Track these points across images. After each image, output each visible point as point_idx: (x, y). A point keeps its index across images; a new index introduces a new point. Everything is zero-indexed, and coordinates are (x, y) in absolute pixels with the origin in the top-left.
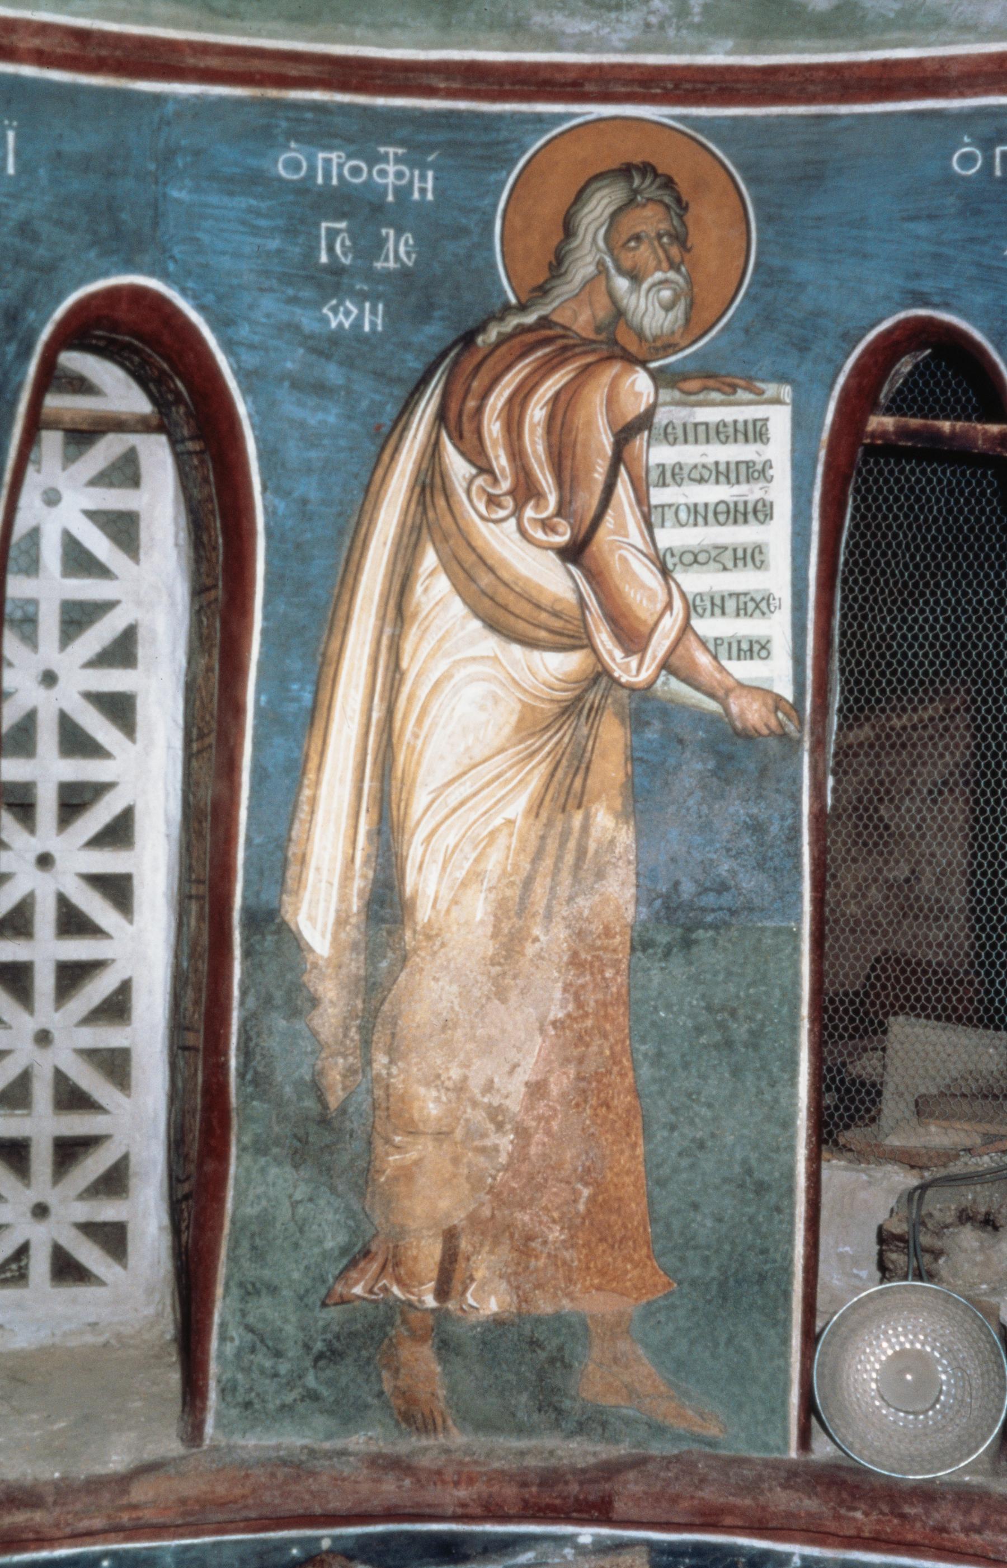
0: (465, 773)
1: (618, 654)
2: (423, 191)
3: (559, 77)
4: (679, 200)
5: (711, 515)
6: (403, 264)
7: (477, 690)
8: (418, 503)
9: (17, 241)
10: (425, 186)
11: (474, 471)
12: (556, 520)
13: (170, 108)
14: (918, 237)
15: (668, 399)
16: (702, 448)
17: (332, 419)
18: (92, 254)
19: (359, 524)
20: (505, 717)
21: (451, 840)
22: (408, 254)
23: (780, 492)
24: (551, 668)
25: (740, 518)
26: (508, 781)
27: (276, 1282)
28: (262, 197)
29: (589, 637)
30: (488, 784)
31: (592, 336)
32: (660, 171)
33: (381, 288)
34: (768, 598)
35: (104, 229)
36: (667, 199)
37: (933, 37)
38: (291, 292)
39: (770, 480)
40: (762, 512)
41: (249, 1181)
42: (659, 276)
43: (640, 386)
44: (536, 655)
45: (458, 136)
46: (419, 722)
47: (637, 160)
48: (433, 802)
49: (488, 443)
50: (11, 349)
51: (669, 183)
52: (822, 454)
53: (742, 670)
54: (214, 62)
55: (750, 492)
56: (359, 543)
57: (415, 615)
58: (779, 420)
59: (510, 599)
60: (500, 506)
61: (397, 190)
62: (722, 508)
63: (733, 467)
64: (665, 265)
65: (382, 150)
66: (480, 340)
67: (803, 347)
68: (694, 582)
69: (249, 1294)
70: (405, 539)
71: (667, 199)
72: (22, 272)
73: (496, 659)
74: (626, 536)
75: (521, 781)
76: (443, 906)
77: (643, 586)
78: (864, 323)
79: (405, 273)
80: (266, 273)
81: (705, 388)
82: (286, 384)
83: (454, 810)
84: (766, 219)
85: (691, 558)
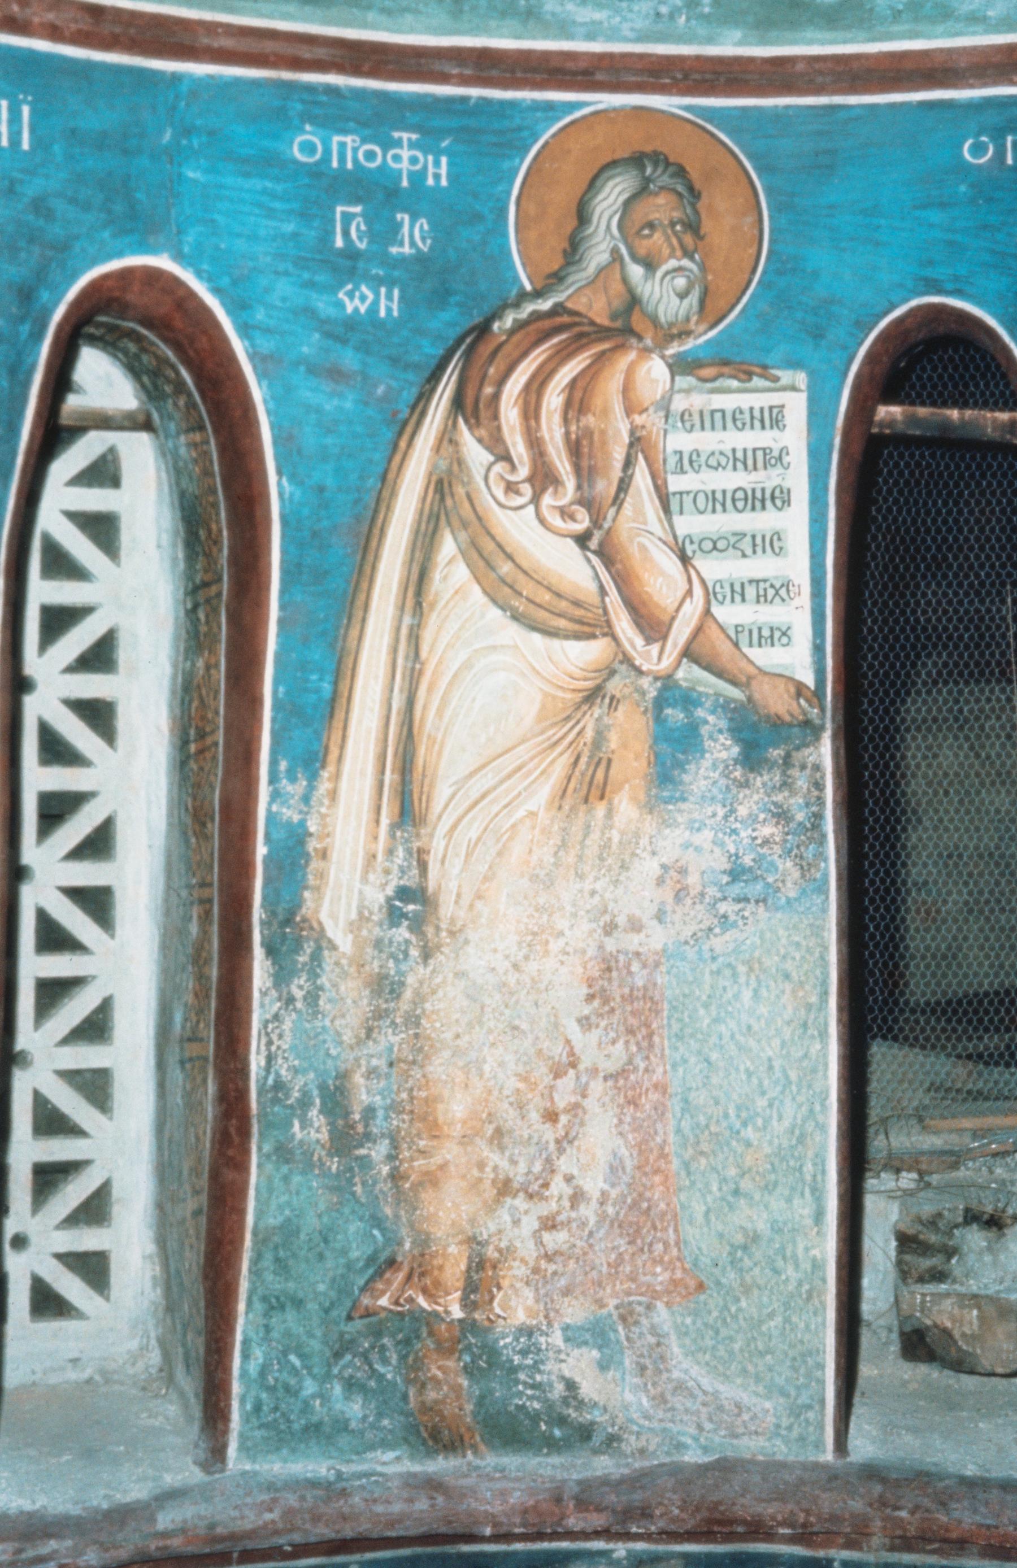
0: (483, 766)
1: (639, 641)
2: (437, 177)
3: (570, 65)
4: (691, 189)
5: (729, 502)
6: (418, 250)
8: (435, 492)
9: (31, 217)
10: (439, 172)
11: (492, 458)
12: (575, 507)
13: (184, 88)
14: (931, 226)
15: (685, 386)
16: (720, 435)
17: (348, 405)
18: (106, 234)
19: (376, 511)
20: (528, 704)
21: (473, 834)
22: (423, 239)
23: (797, 479)
25: (758, 504)
26: (530, 773)
27: (301, 1294)
28: (278, 180)
29: (609, 623)
30: (509, 776)
32: (671, 160)
33: (396, 273)
34: (787, 585)
35: (119, 208)
36: (680, 188)
37: (940, 29)
38: (306, 276)
40: (780, 498)
41: (271, 1190)
42: (673, 263)
43: (655, 372)
44: (556, 643)
45: (472, 122)
46: (440, 713)
47: (648, 149)
49: (505, 429)
50: (25, 329)
51: (681, 172)
52: (837, 441)
53: (765, 657)
54: (227, 43)
55: (768, 479)
56: (376, 531)
57: (432, 606)
58: (796, 407)
59: (528, 589)
60: (518, 493)
61: (411, 175)
62: (740, 495)
63: (750, 454)
64: (679, 253)
65: (396, 135)
66: (496, 326)
67: (817, 335)
68: (713, 568)
69: (273, 1308)
71: (680, 188)
72: (36, 250)
73: (516, 647)
74: (645, 523)
75: (542, 773)
76: (466, 900)
77: (662, 573)
78: (878, 309)
79: (420, 259)
80: (281, 256)
81: (721, 375)
82: (302, 368)
83: (476, 803)
84: (776, 209)
85: (710, 545)
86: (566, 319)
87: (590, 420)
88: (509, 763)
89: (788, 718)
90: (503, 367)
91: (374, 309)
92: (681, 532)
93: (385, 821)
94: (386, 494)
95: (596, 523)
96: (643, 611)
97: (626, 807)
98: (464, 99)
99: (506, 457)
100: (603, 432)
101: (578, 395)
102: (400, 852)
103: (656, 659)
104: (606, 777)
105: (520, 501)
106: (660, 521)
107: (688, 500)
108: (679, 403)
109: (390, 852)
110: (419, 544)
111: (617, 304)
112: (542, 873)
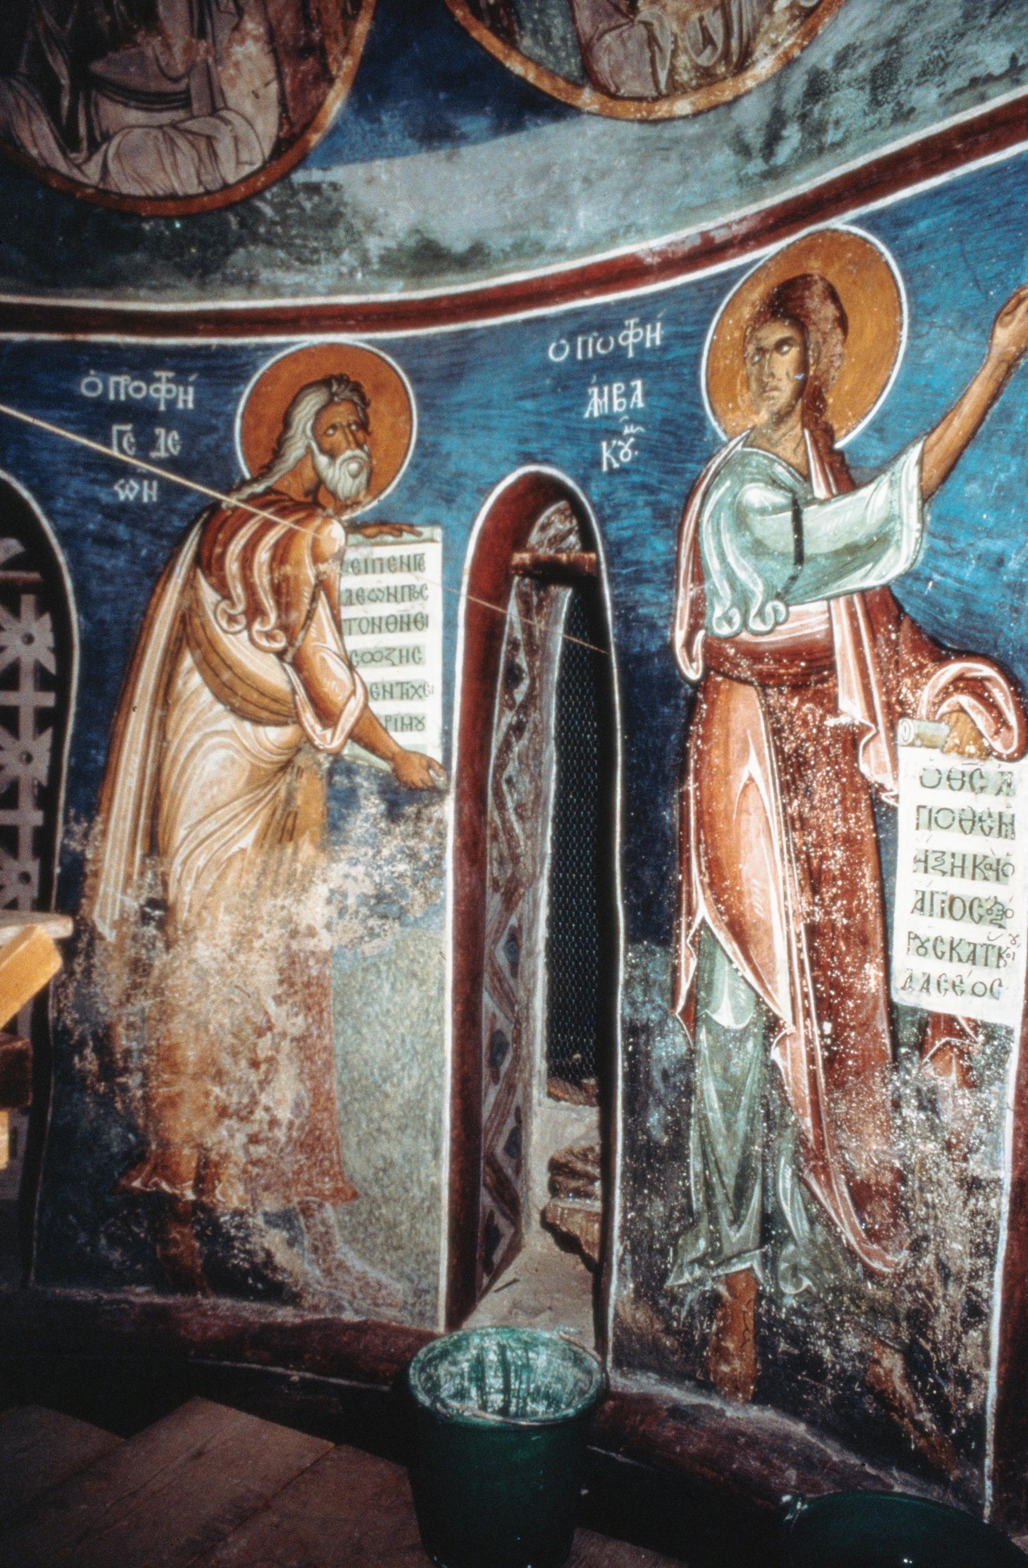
1: (318, 728)
4: (363, 398)
7: (221, 754)
10: (187, 399)
16: (377, 577)
21: (201, 863)
23: (434, 607)
28: (71, 409)
29: (298, 715)
31: (302, 499)
36: (356, 399)
37: (536, 261)
38: (92, 475)
39: (426, 599)
40: (419, 622)
42: (348, 453)
44: (261, 729)
45: (212, 362)
47: (336, 372)
49: (229, 580)
53: (404, 739)
58: (433, 554)
60: (236, 622)
65: (157, 374)
67: (449, 500)
68: (369, 674)
76: (196, 908)
77: (335, 678)
81: (381, 533)
84: (424, 407)
86: (273, 497)
87: (288, 569)
89: (420, 784)
93: (139, 852)
95: (291, 643)
97: (307, 849)
98: (208, 347)
100: (296, 578)
101: (280, 552)
102: (149, 875)
103: (330, 739)
108: (351, 555)
109: (142, 874)
111: (308, 485)
112: (248, 892)
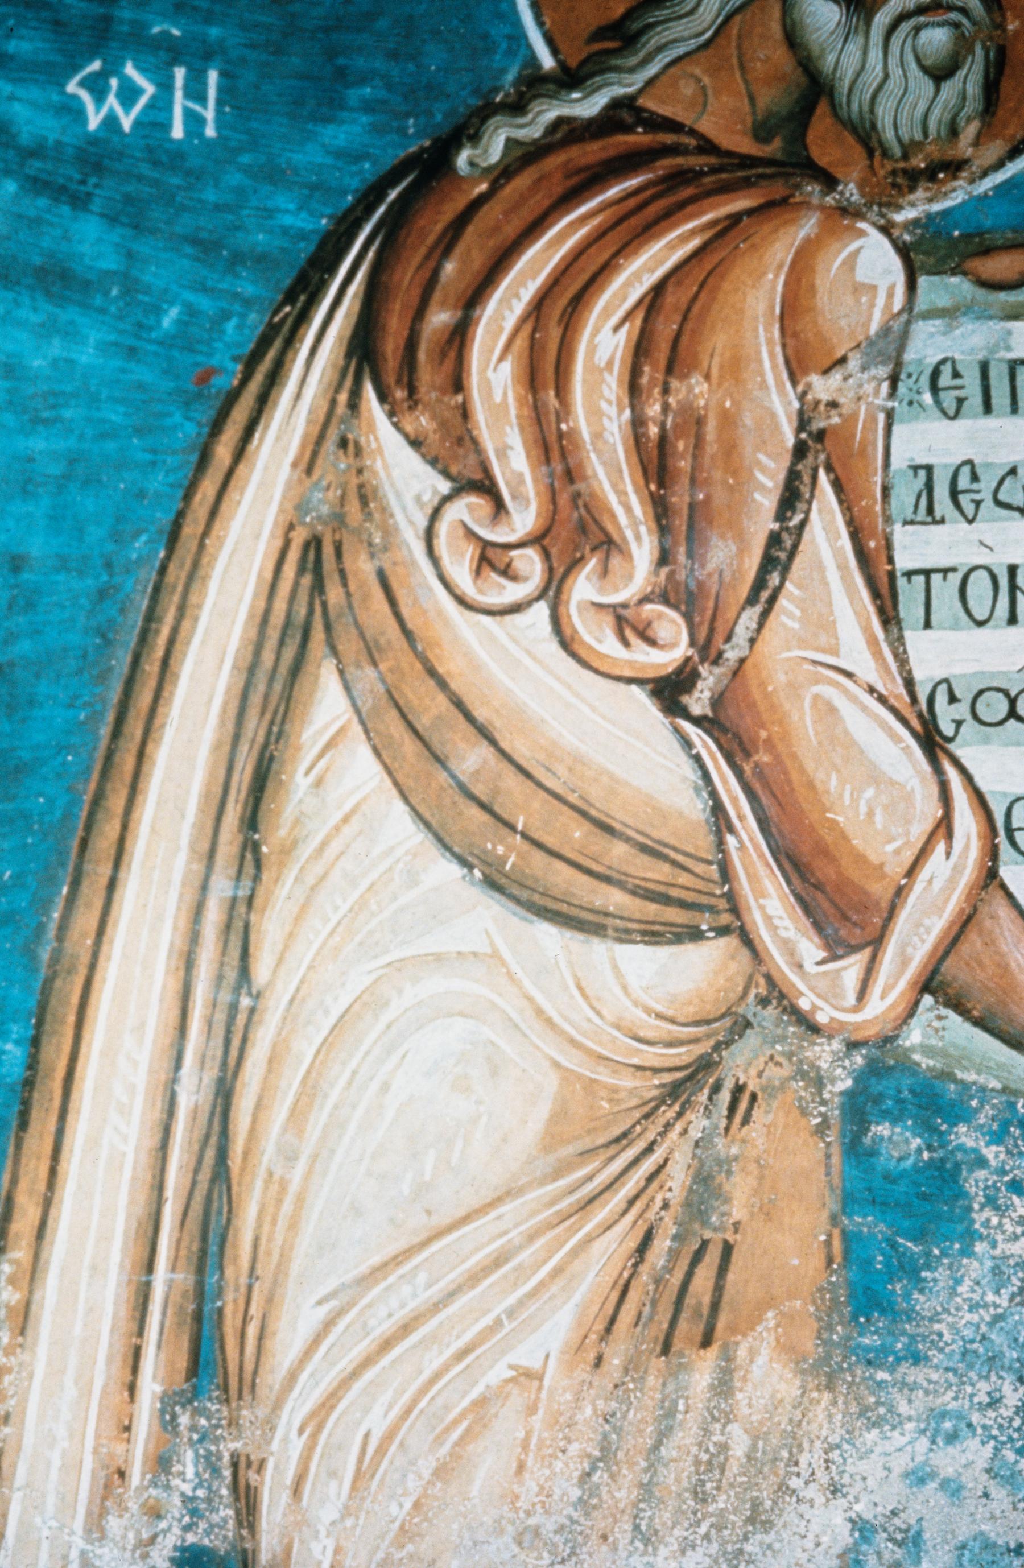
8: (301, 570)
11: (445, 487)
15: (943, 301)
17: (86, 356)
19: (151, 617)
20: (507, 1118)
21: (377, 1422)
24: (634, 982)
26: (523, 1273)
29: (734, 905)
30: (474, 1279)
31: (746, 146)
33: (214, 32)
44: (599, 950)
46: (298, 1116)
48: (328, 1324)
49: (480, 414)
56: (151, 667)
57: (287, 851)
59: (528, 810)
60: (507, 572)
66: (462, 160)
70: (268, 657)
73: (495, 954)
74: (835, 652)
75: (557, 1272)
77: (876, 777)
83: (386, 1345)
85: (1004, 707)
86: (639, 138)
87: (696, 390)
88: (477, 1242)
90: (479, 261)
91: (154, 122)
92: (924, 674)
93: (150, 1387)
94: (176, 574)
95: (707, 650)
96: (825, 872)
97: (767, 1374)
99: (485, 486)
100: (728, 420)
101: (666, 328)
102: (188, 1464)
103: (856, 996)
104: (719, 1288)
105: (513, 592)
106: (872, 642)
107: (945, 591)
108: (927, 344)
109: (162, 1464)
110: (256, 699)
111: (771, 98)
112: (549, 1525)
